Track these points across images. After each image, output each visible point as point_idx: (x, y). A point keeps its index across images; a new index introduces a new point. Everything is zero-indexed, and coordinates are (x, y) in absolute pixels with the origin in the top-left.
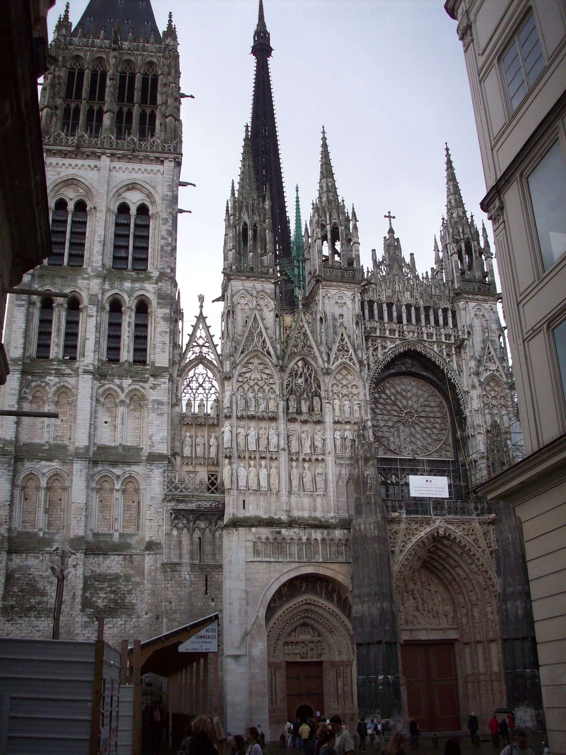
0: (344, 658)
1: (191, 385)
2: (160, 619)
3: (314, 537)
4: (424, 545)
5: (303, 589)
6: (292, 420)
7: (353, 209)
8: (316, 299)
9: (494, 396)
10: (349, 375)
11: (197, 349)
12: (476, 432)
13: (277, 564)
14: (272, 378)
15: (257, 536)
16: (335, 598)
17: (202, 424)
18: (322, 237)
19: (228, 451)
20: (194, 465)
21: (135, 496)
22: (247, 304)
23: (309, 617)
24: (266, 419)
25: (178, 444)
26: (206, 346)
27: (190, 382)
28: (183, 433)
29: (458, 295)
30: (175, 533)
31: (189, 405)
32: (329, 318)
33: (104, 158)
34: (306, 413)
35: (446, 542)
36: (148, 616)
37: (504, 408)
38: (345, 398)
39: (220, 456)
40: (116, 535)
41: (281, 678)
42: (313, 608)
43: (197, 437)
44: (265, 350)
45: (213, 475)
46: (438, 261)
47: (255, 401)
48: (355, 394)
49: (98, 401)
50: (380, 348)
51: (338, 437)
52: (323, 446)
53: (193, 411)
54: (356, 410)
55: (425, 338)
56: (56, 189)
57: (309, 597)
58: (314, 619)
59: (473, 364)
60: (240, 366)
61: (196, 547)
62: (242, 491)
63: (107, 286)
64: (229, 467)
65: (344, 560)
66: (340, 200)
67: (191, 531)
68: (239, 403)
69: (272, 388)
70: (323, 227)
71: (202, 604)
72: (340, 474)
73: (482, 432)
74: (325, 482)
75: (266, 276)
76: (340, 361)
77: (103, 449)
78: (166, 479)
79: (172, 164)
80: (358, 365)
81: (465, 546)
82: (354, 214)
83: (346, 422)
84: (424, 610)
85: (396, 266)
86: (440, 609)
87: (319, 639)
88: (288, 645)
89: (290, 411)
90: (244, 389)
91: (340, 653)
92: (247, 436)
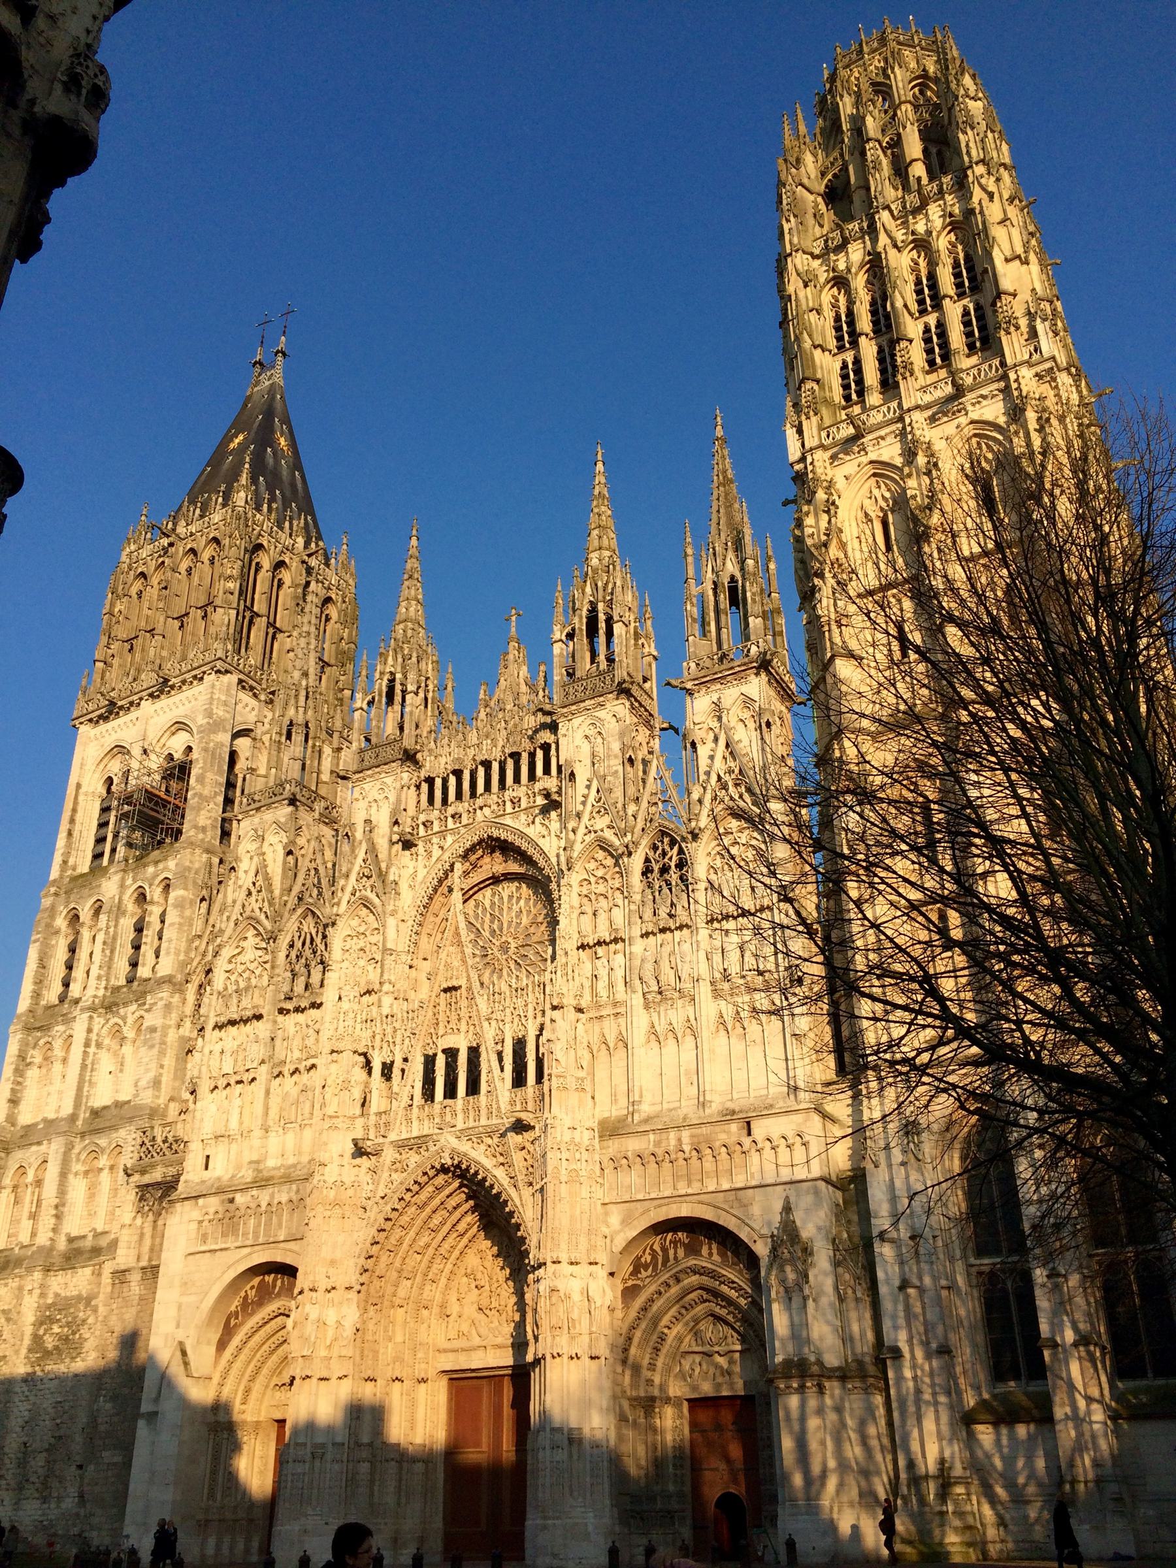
3: (276, 1202)
6: (281, 1011)
13: (224, 1253)
15: (204, 1211)
30: (139, 1221)
33: (143, 702)
40: (90, 1238)
49: (99, 1045)
56: (102, 766)
63: (129, 882)
77: (96, 1113)
79: (213, 676)
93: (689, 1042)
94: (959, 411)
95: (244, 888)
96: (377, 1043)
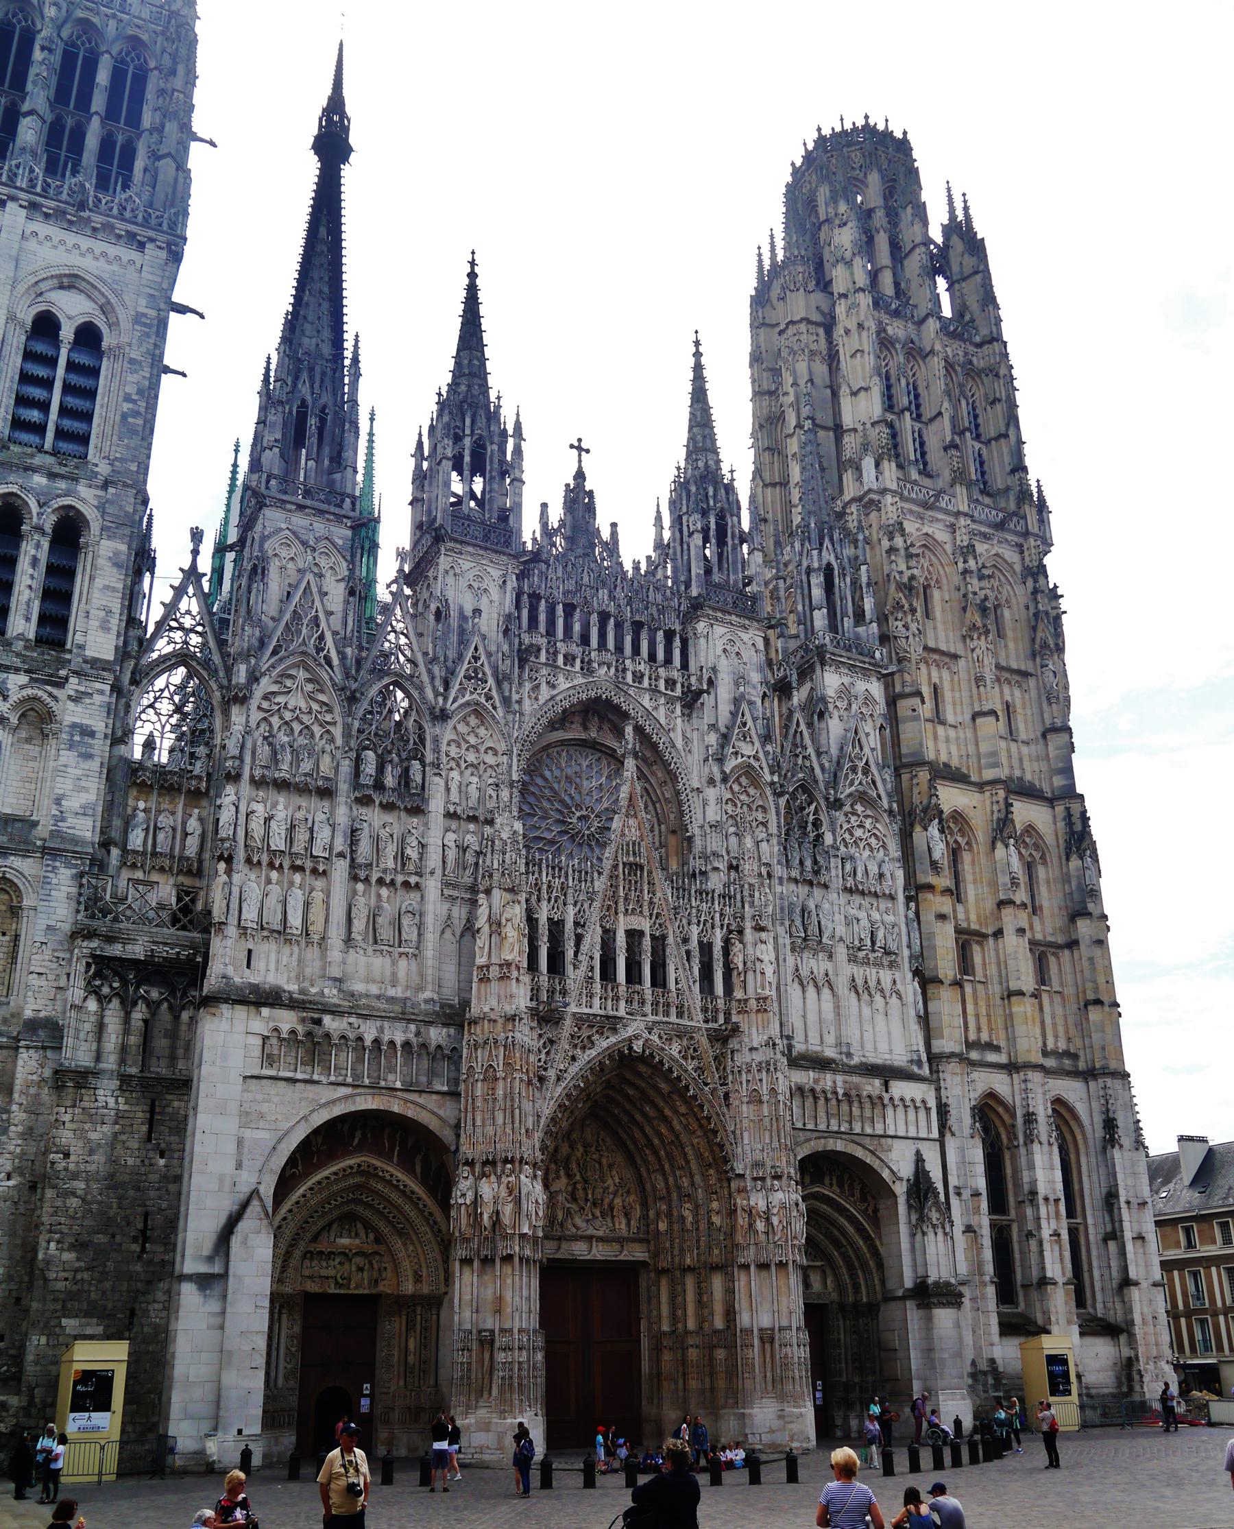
0: (425, 1289)
1: (157, 705)
2: (39, 1191)
3: (386, 1038)
4: (602, 1070)
5: (356, 1141)
6: (365, 801)
7: (518, 415)
8: (430, 574)
10: (482, 728)
11: (178, 636)
12: (709, 867)
13: (309, 1087)
14: (330, 711)
15: (271, 1025)
16: (418, 1169)
17: (173, 789)
18: (454, 456)
19: (227, 845)
20: (147, 869)
21: (9, 921)
22: (292, 559)
23: (361, 1201)
24: (311, 791)
25: (117, 822)
26: (197, 632)
27: (156, 699)
28: (131, 802)
29: (696, 606)
30: (92, 1005)
31: (149, 745)
32: (454, 613)
34: (394, 790)
35: (642, 1068)
36: (11, 1183)
37: (761, 827)
38: (470, 770)
39: (207, 855)
41: (291, 1327)
42: (373, 1183)
43: (159, 812)
44: (322, 655)
45: (187, 894)
46: (659, 545)
47: (292, 753)
48: (491, 766)
50: (544, 687)
51: (452, 844)
52: (421, 859)
53: (156, 758)
54: (490, 797)
55: (629, 678)
57: (363, 1159)
58: (370, 1206)
59: (712, 739)
61: (133, 1040)
62: (249, 931)
64: (224, 878)
65: (445, 1088)
66: (493, 398)
67: (128, 1006)
68: (259, 751)
69: (328, 731)
70: (458, 439)
71: (138, 1161)
72: (449, 917)
73: (721, 867)
74: (419, 929)
75: (337, 510)
76: (467, 697)
78: (85, 891)
80: (500, 712)
81: (679, 1078)
82: (518, 426)
83: (468, 817)
84: (587, 1200)
85: (583, 541)
86: (618, 1201)
87: (376, 1247)
88: (311, 1260)
89: (363, 781)
90: (271, 725)
91: (418, 1279)
92: (268, 820)
93: (826, 992)
94: (989, 539)
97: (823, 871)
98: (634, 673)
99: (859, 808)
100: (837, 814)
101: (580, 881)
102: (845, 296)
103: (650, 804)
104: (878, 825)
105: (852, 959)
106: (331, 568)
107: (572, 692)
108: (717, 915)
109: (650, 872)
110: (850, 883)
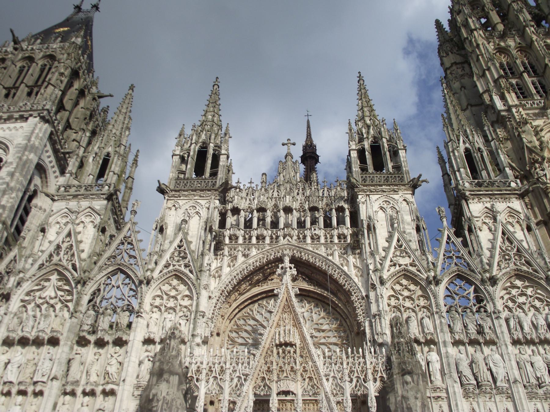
6: (82, 342)
9: (408, 297)
34: (101, 331)
48: (186, 307)
55: (309, 240)
60: (30, 282)
69: (67, 306)
95: (55, 243)
96: (203, 376)
97: (487, 330)
98: (312, 238)
99: (518, 283)
100: (495, 287)
101: (238, 364)
102: (467, 38)
103: (344, 322)
104: (539, 291)
105: (531, 396)
106: (92, 222)
107: (261, 256)
108: (370, 372)
109: (302, 348)
110: (518, 335)
